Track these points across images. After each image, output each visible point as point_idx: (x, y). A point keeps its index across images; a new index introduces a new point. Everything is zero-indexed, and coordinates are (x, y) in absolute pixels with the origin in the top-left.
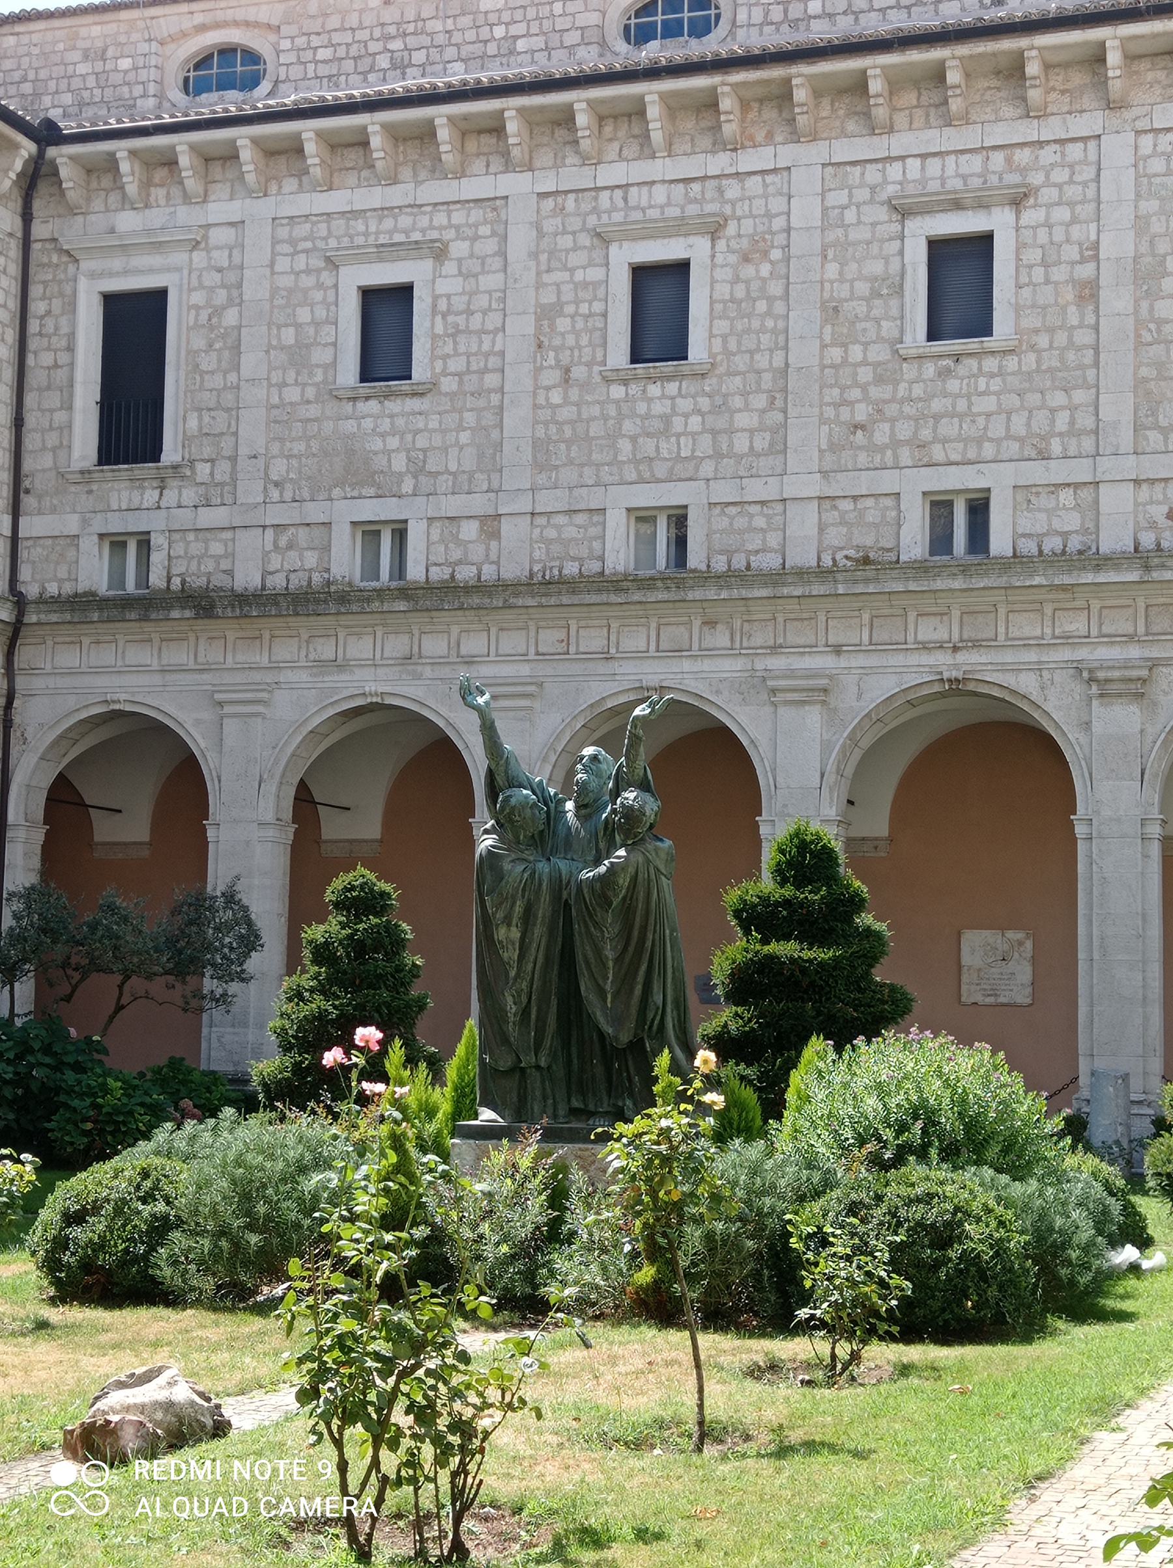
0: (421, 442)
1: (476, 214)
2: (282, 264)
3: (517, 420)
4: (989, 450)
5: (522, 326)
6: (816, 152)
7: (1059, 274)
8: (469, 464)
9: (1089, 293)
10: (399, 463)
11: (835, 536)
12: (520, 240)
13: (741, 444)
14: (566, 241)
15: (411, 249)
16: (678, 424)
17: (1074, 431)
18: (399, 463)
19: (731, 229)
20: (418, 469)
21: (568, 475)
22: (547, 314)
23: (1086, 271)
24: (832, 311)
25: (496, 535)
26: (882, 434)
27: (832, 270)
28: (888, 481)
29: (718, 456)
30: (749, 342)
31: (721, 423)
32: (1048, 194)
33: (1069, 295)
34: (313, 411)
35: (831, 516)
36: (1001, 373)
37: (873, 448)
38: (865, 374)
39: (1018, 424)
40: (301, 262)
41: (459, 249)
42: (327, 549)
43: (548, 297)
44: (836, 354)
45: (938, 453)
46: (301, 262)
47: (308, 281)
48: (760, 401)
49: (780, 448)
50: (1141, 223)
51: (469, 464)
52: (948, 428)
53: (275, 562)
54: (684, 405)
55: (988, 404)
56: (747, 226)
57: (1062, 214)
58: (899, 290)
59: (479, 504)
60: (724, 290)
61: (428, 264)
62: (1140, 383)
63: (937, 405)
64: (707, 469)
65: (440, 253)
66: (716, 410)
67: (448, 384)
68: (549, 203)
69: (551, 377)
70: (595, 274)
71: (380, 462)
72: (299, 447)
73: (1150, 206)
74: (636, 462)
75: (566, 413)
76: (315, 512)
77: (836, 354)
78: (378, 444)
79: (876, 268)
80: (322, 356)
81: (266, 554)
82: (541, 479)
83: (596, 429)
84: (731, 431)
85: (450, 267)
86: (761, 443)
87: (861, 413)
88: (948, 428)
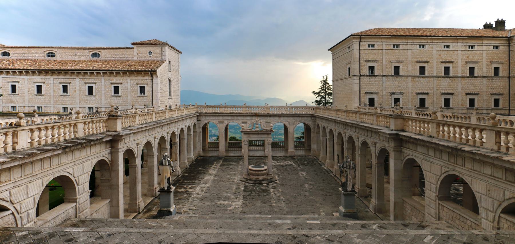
0: (18, 99)
1: (22, 79)
2: (3, 82)
3: (26, 98)
4: (68, 104)
5: (27, 90)
6: (53, 77)
7: (73, 89)
8: (22, 101)
9: (75, 91)
10: (15, 101)
11: (55, 110)
12: (26, 82)
13: (47, 101)
14: (31, 82)
15: (16, 82)
16: (41, 99)
17: (74, 103)
18: (15, 101)
19: (45, 83)
20: (17, 102)
21: (31, 103)
22: (29, 89)
23: (75, 89)
24: (54, 91)
25: (25, 108)
26: (59, 102)
27: (54, 87)
28: (59, 106)
29: (45, 102)
30: (47, 93)
31: (45, 99)
32: (72, 83)
33: (74, 91)
34: (7, 96)
35: (55, 108)
36: (68, 97)
37: (58, 103)
38: (57, 96)
39: (70, 102)
40: (5, 82)
41: (20, 82)
42: (9, 108)
43: (29, 87)
44: (55, 94)
45: (63, 104)
46: (5, 82)
47: (6, 83)
48: (48, 98)
49: (50, 102)
50: (79, 86)
51: (22, 101)
52: (64, 101)
53: (4, 109)
54: (42, 98)
55: (67, 100)
56: (47, 83)
57: (73, 85)
58: (60, 90)
59: (23, 105)
60: (45, 88)
61: (17, 83)
62: (79, 99)
63: (64, 100)
64: (44, 103)
65: (19, 82)
66: (45, 98)
67: (20, 94)
68: (29, 79)
69: (30, 94)
70: (33, 86)
71: (14, 101)
72: (6, 99)
73: (80, 85)
74: (38, 102)
75: (31, 98)
76: (7, 105)
77: (55, 94)
78: (13, 99)
79: (58, 87)
80: (7, 90)
81: (3, 109)
82: (29, 103)
83: (34, 99)
84: (46, 100)
85: (20, 84)
86: (49, 101)
87: (57, 100)
88: (64, 101)
